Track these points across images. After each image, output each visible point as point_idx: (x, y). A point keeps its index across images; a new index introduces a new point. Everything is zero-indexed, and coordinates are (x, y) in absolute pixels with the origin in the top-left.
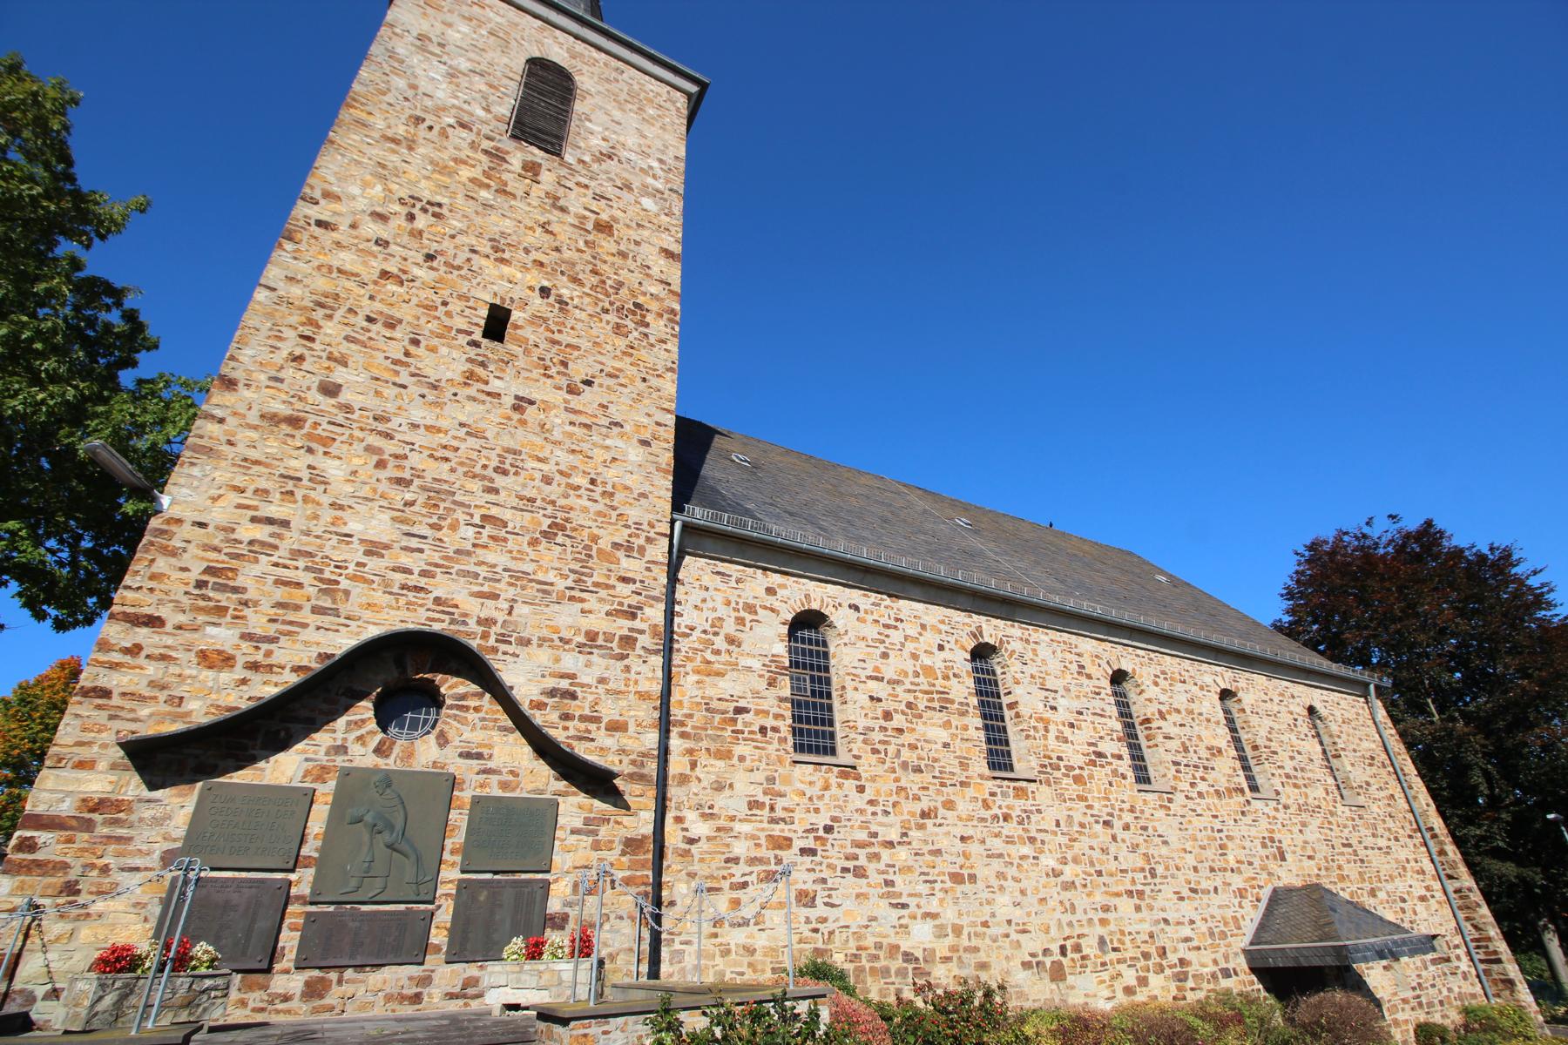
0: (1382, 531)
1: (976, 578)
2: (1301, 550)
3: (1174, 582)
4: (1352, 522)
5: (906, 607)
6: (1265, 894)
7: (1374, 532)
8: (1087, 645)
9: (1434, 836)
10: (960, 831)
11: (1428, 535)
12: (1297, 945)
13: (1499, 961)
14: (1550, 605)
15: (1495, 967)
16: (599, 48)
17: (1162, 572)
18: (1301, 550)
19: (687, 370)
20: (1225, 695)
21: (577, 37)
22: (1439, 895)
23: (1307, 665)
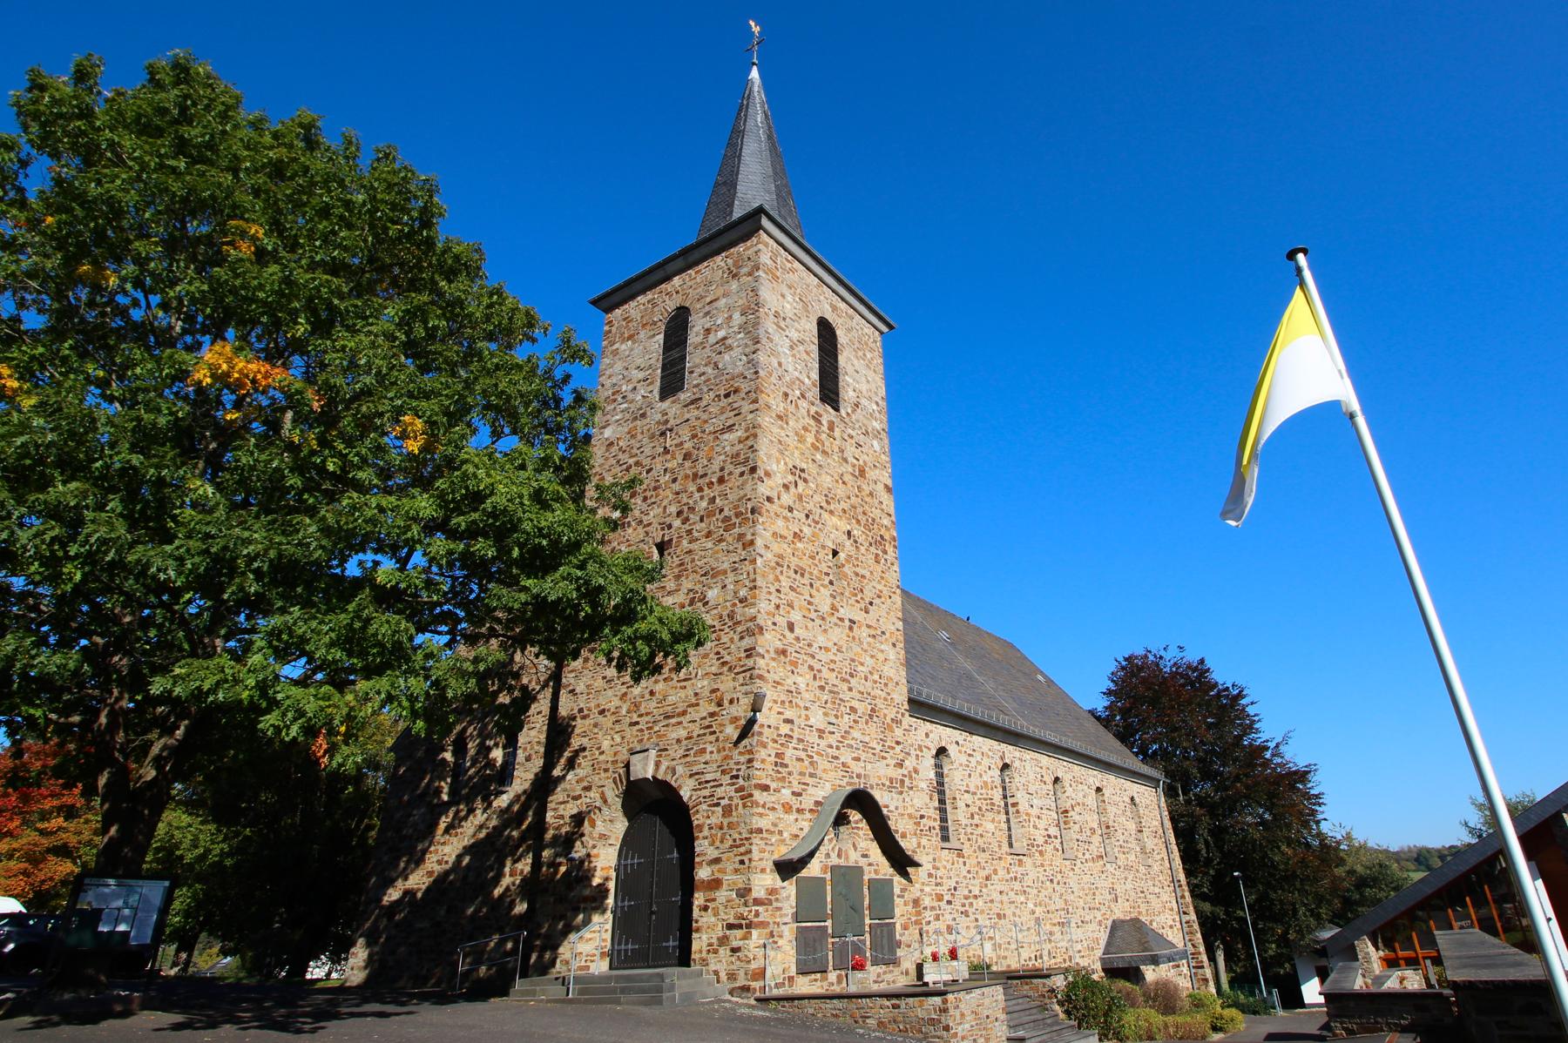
0: (1171, 656)
1: (1003, 721)
2: (1121, 659)
3: (1050, 682)
4: (1156, 647)
5: (978, 740)
6: (1109, 923)
7: (1167, 656)
8: (1045, 760)
9: (1180, 886)
10: (999, 888)
11: (1201, 669)
12: (1126, 956)
13: (1202, 967)
14: (1258, 731)
15: (1200, 971)
16: (843, 299)
17: (1042, 673)
18: (1121, 659)
20: (1099, 790)
21: (833, 291)
22: (1178, 924)
23: (1141, 771)
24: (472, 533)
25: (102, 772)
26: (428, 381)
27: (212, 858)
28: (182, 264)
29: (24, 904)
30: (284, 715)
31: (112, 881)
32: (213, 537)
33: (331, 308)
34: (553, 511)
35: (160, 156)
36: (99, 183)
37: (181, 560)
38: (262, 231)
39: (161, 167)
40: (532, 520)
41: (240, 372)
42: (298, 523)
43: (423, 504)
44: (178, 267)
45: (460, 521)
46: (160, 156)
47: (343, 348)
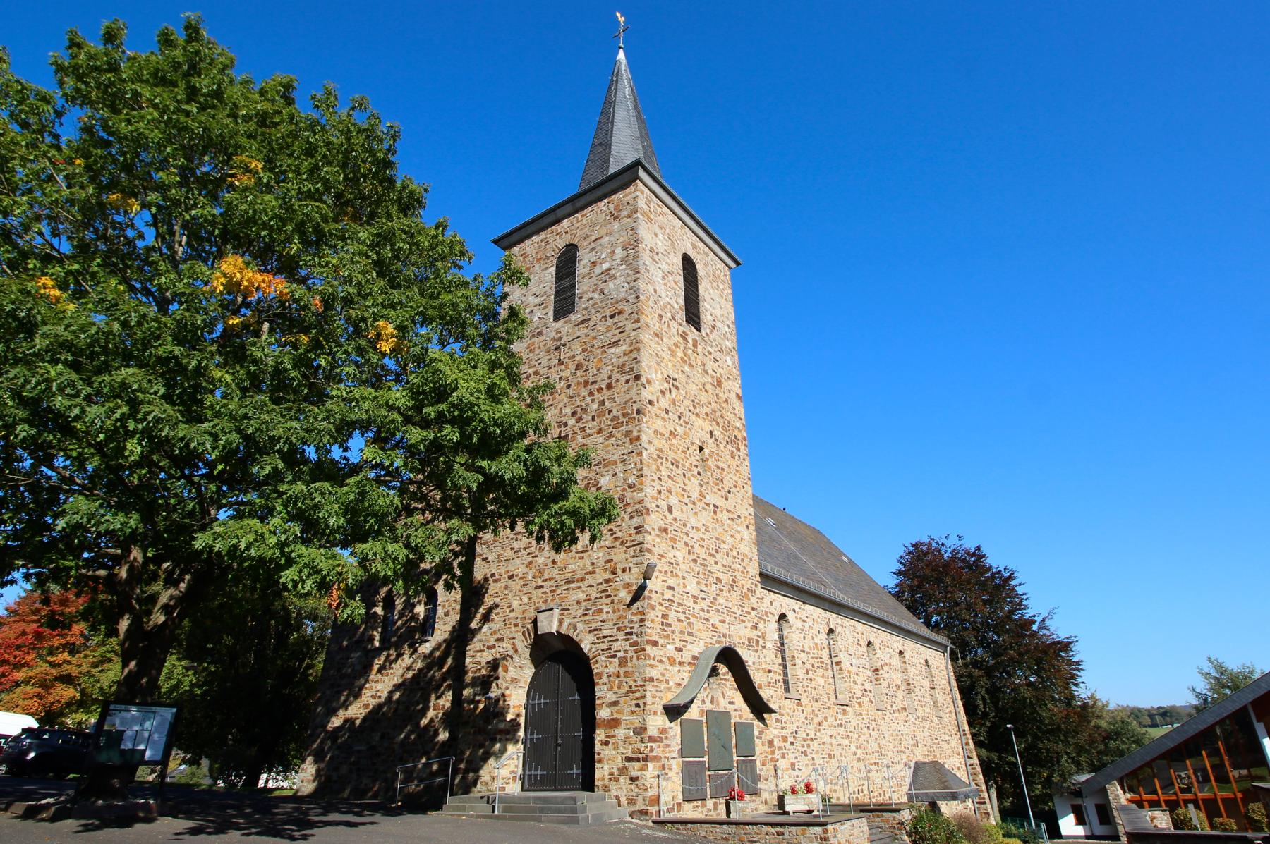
6: (912, 764)
8: (860, 627)
9: (965, 735)
13: (984, 803)
16: (701, 239)
19: (754, 477)
20: (901, 653)
24: (441, 419)
25: (122, 616)
26: (396, 295)
27: (185, 687)
28: (196, 192)
29: (39, 720)
30: (300, 571)
31: (134, 708)
32: (250, 419)
33: (317, 230)
34: (502, 404)
35: (177, 101)
36: (129, 122)
37: (215, 437)
38: (260, 166)
39: (178, 110)
40: (487, 412)
41: (249, 280)
42: (309, 411)
43: (398, 395)
44: (193, 194)
45: (430, 411)
46: (177, 101)
47: (327, 264)
